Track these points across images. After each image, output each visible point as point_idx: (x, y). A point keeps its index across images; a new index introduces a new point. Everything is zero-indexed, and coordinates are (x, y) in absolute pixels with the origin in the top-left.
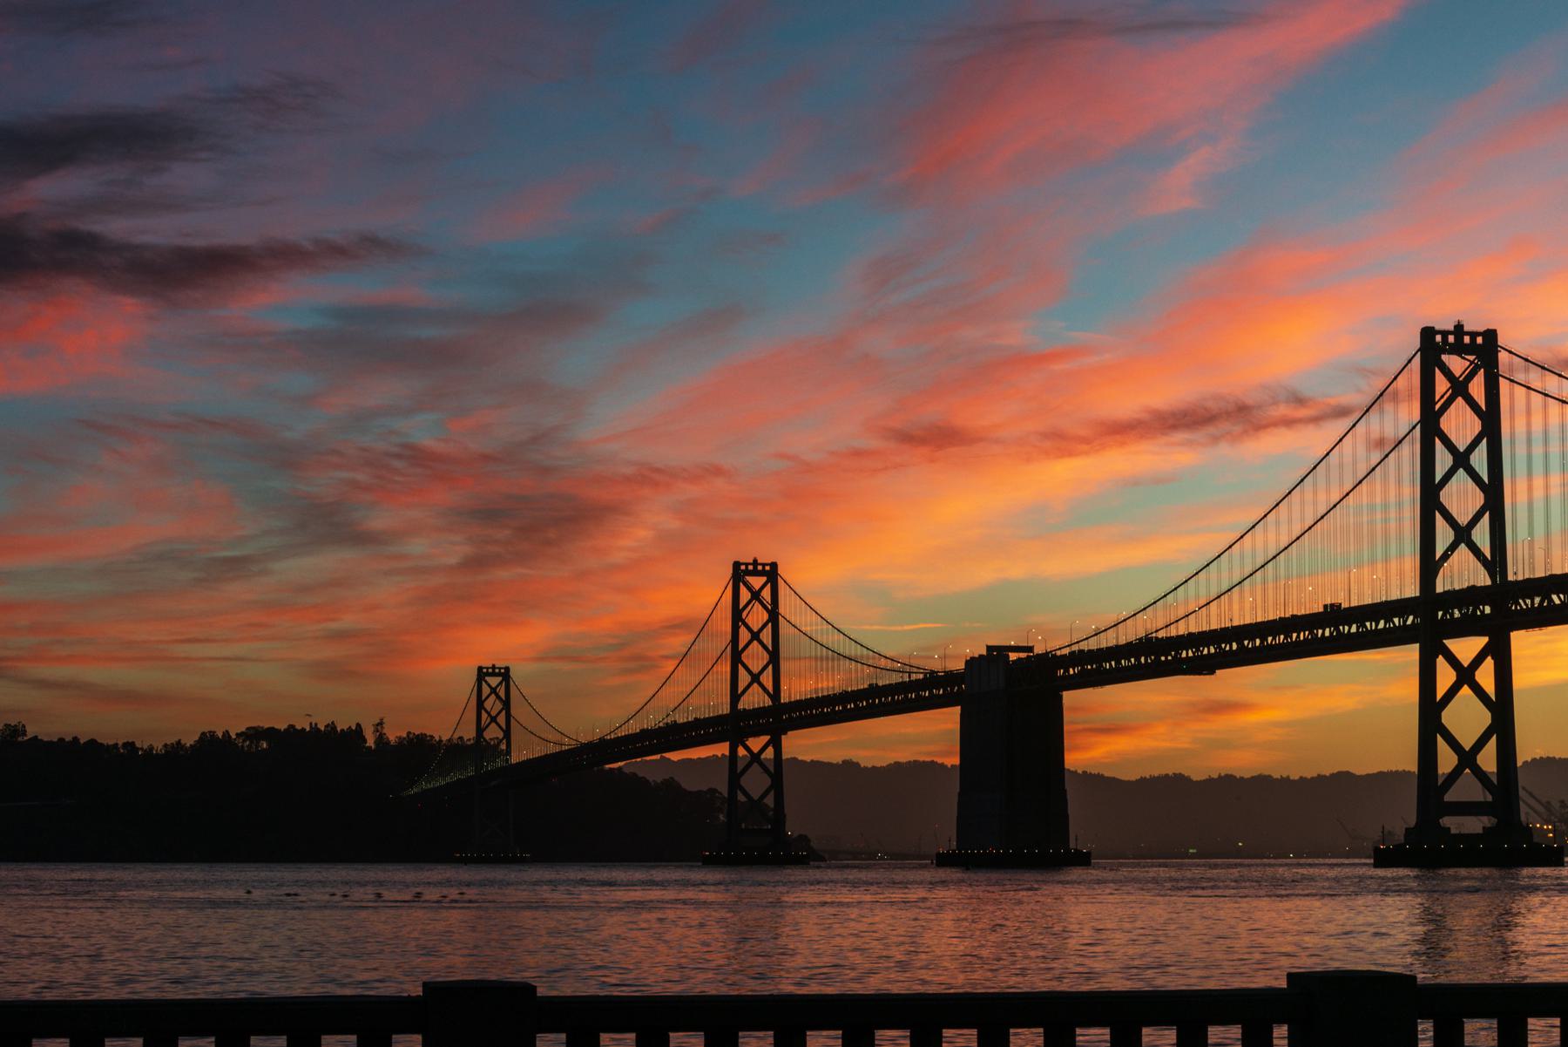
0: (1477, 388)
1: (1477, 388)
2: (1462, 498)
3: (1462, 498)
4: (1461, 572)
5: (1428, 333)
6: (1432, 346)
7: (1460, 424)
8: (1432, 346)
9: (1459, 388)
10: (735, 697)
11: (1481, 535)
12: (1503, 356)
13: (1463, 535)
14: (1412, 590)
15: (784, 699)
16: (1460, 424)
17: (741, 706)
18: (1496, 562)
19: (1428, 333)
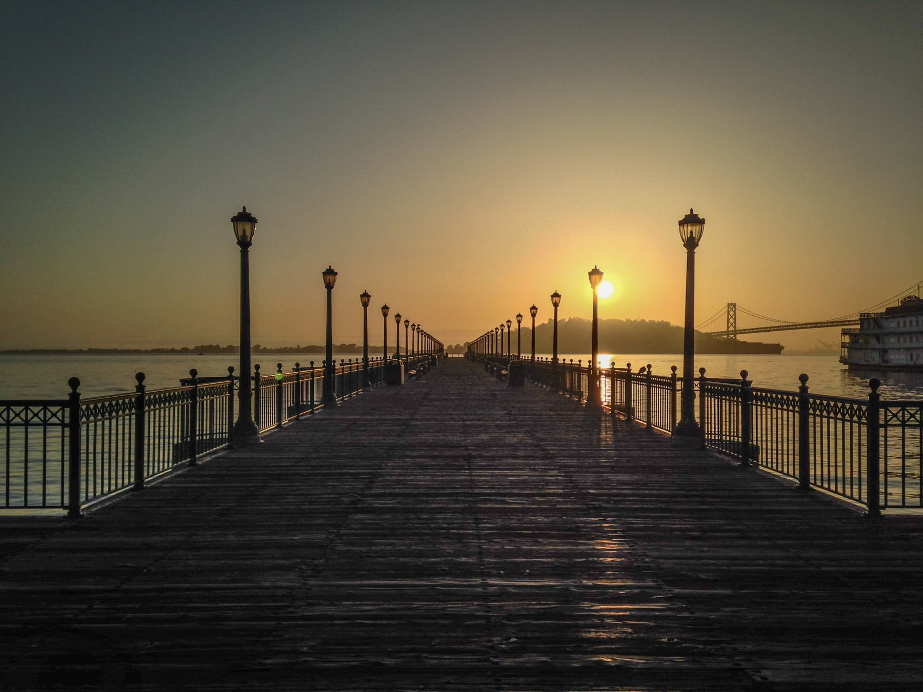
0: (733, 309)
1: (733, 309)
2: (732, 321)
3: (732, 321)
4: (732, 329)
5: (728, 304)
6: (729, 305)
7: (732, 313)
8: (729, 305)
9: (732, 309)
10: (728, 327)
11: (734, 325)
12: (737, 307)
13: (732, 325)
14: (726, 330)
15: (737, 329)
16: (732, 313)
17: (730, 330)
18: (735, 327)
19: (728, 304)
